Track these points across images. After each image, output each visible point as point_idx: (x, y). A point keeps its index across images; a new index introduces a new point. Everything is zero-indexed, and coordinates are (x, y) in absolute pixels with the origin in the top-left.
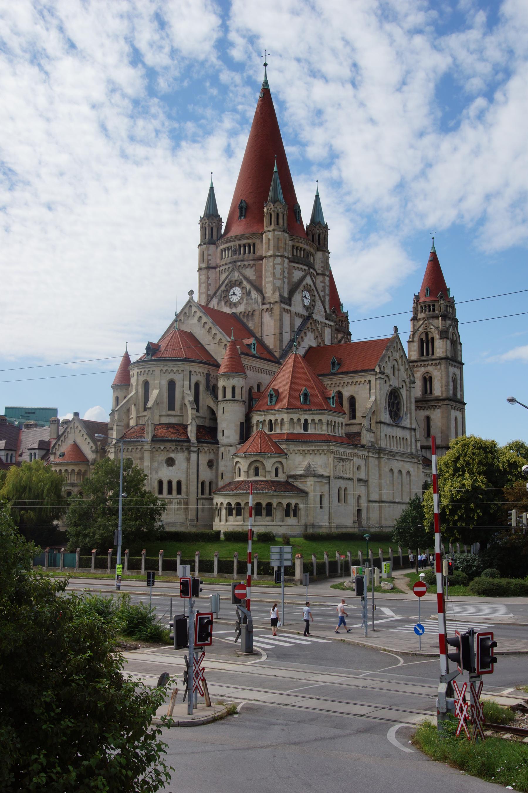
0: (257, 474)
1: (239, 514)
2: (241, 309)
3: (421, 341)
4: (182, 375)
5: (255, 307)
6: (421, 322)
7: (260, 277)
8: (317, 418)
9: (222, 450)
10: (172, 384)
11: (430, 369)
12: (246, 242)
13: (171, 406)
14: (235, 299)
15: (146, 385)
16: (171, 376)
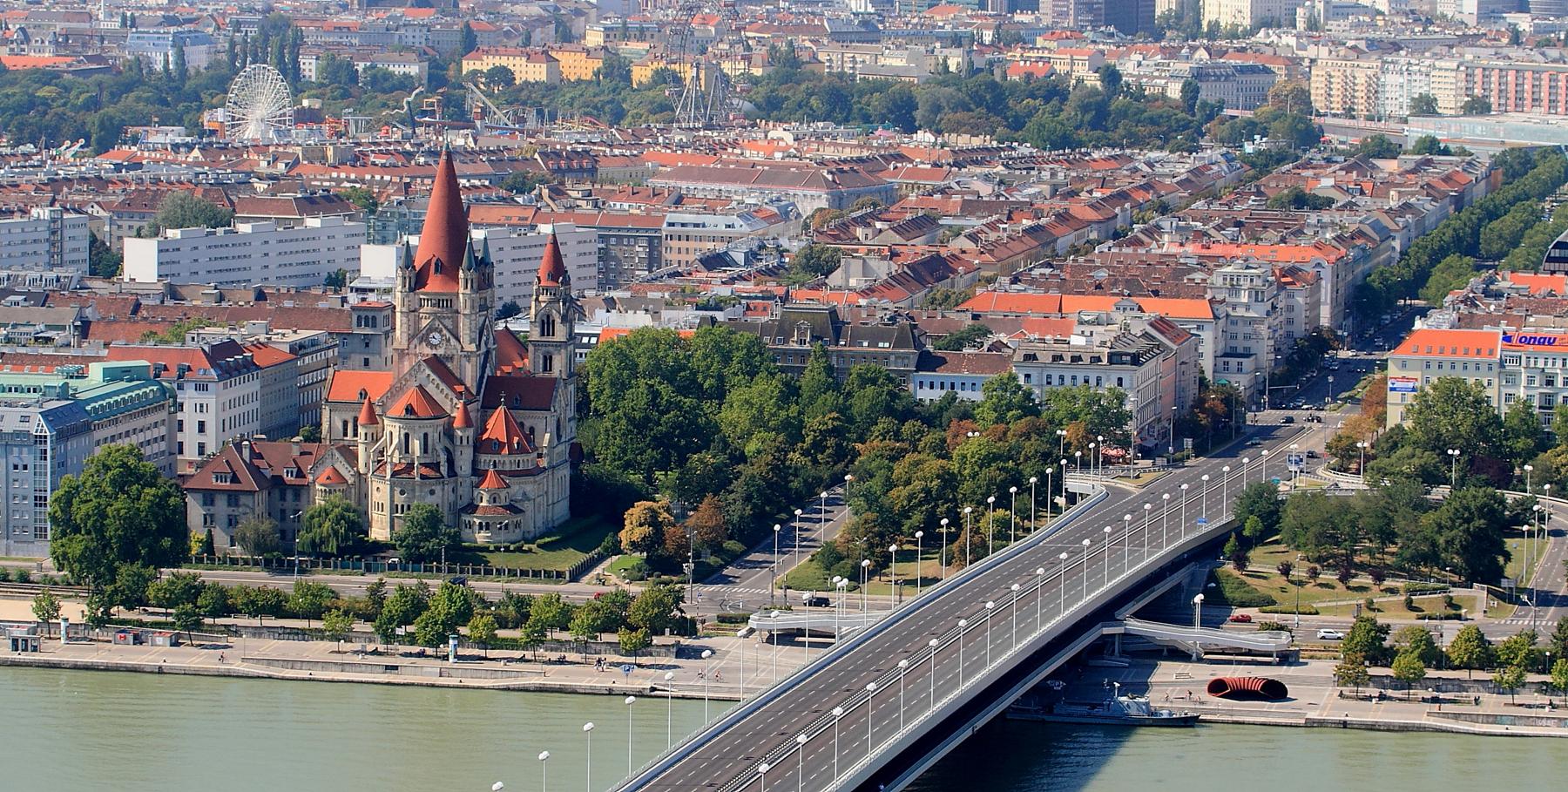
0: (495, 502)
1: (487, 529)
2: (440, 352)
3: (543, 321)
4: (431, 429)
5: (454, 352)
6: (543, 305)
7: (457, 327)
8: (525, 458)
9: (460, 480)
10: (426, 435)
11: (551, 349)
12: (445, 298)
13: (426, 451)
14: (434, 342)
15: (407, 436)
16: (426, 430)
